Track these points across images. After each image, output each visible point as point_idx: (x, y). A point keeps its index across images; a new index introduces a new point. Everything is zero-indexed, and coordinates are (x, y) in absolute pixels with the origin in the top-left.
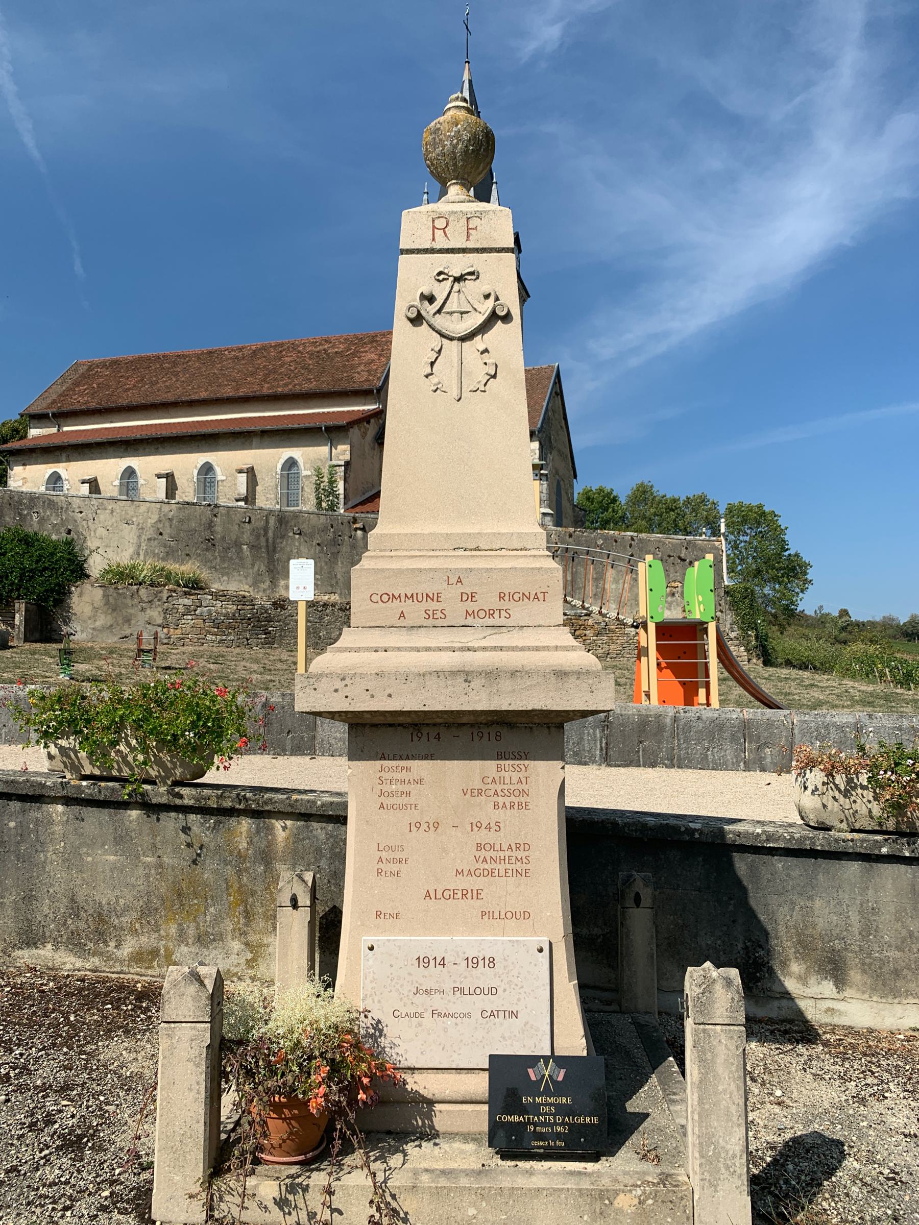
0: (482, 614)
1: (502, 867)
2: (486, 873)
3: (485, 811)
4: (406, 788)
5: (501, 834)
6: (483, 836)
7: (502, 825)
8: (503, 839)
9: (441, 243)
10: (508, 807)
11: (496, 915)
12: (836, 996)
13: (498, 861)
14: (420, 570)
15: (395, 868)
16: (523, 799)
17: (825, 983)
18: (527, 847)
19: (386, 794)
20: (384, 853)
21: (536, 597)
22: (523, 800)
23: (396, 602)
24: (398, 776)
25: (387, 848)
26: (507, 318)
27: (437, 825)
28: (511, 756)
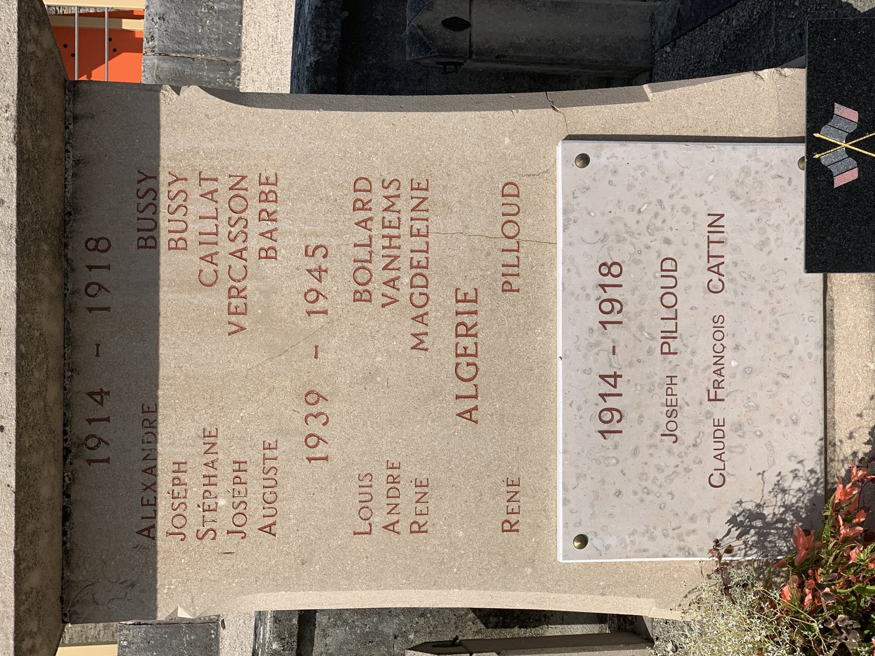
1: (407, 244)
2: (419, 281)
3: (278, 281)
4: (225, 471)
5: (332, 243)
6: (338, 286)
7: (313, 242)
8: (344, 239)
10: (271, 225)
11: (510, 258)
13: (395, 252)
15: (408, 493)
16: (253, 190)
19: (240, 520)
20: (376, 519)
22: (253, 190)
24: (195, 491)
25: (365, 513)
27: (313, 396)
28: (148, 214)
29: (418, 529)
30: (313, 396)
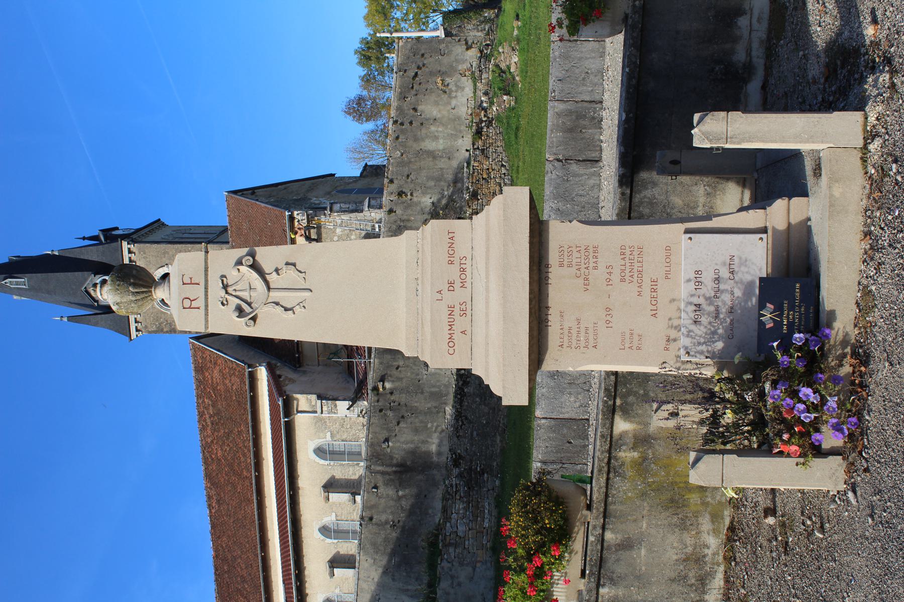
0: (463, 276)
1: (636, 265)
3: (598, 276)
4: (583, 330)
6: (616, 277)
7: (609, 264)
9: (200, 303)
11: (668, 269)
12: (748, 16)
15: (636, 338)
16: (591, 250)
17: (739, 24)
18: (623, 247)
21: (451, 238)
22: (591, 250)
23: (454, 336)
24: (575, 335)
26: (252, 254)
27: (608, 309)
29: (639, 348)
30: (608, 309)
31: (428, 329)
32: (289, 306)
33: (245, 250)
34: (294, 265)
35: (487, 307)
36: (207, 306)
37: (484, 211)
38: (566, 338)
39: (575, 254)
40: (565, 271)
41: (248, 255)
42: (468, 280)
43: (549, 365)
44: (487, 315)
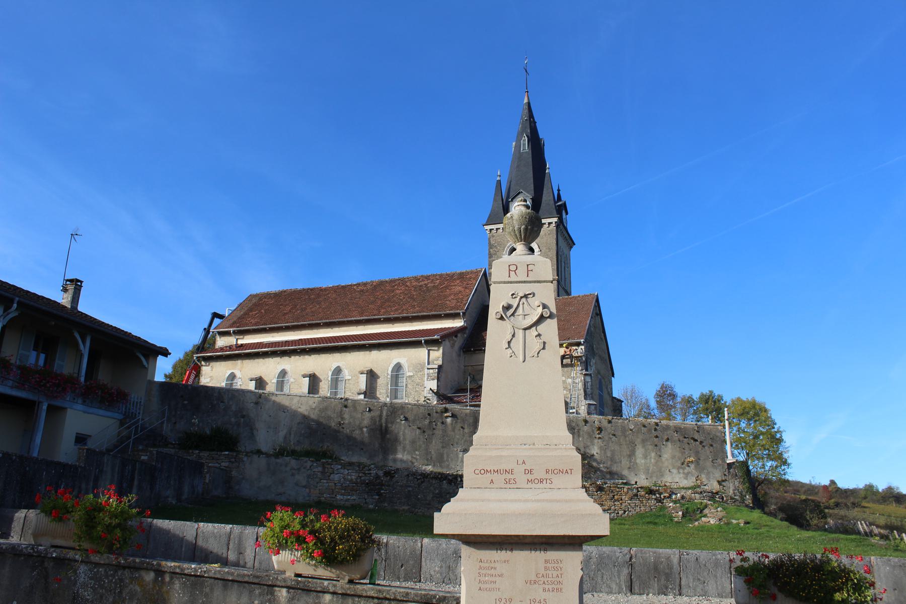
0: (536, 481)
4: (494, 579)
9: (513, 278)
14: (501, 456)
16: (558, 586)
22: (558, 586)
24: (489, 572)
26: (551, 316)
31: (494, 453)
32: (512, 345)
33: (554, 311)
34: (544, 348)
35: (512, 501)
36: (511, 282)
37: (588, 498)
38: (487, 565)
39: (555, 573)
40: (542, 565)
41: (551, 313)
42: (534, 485)
43: (465, 550)
44: (506, 501)
